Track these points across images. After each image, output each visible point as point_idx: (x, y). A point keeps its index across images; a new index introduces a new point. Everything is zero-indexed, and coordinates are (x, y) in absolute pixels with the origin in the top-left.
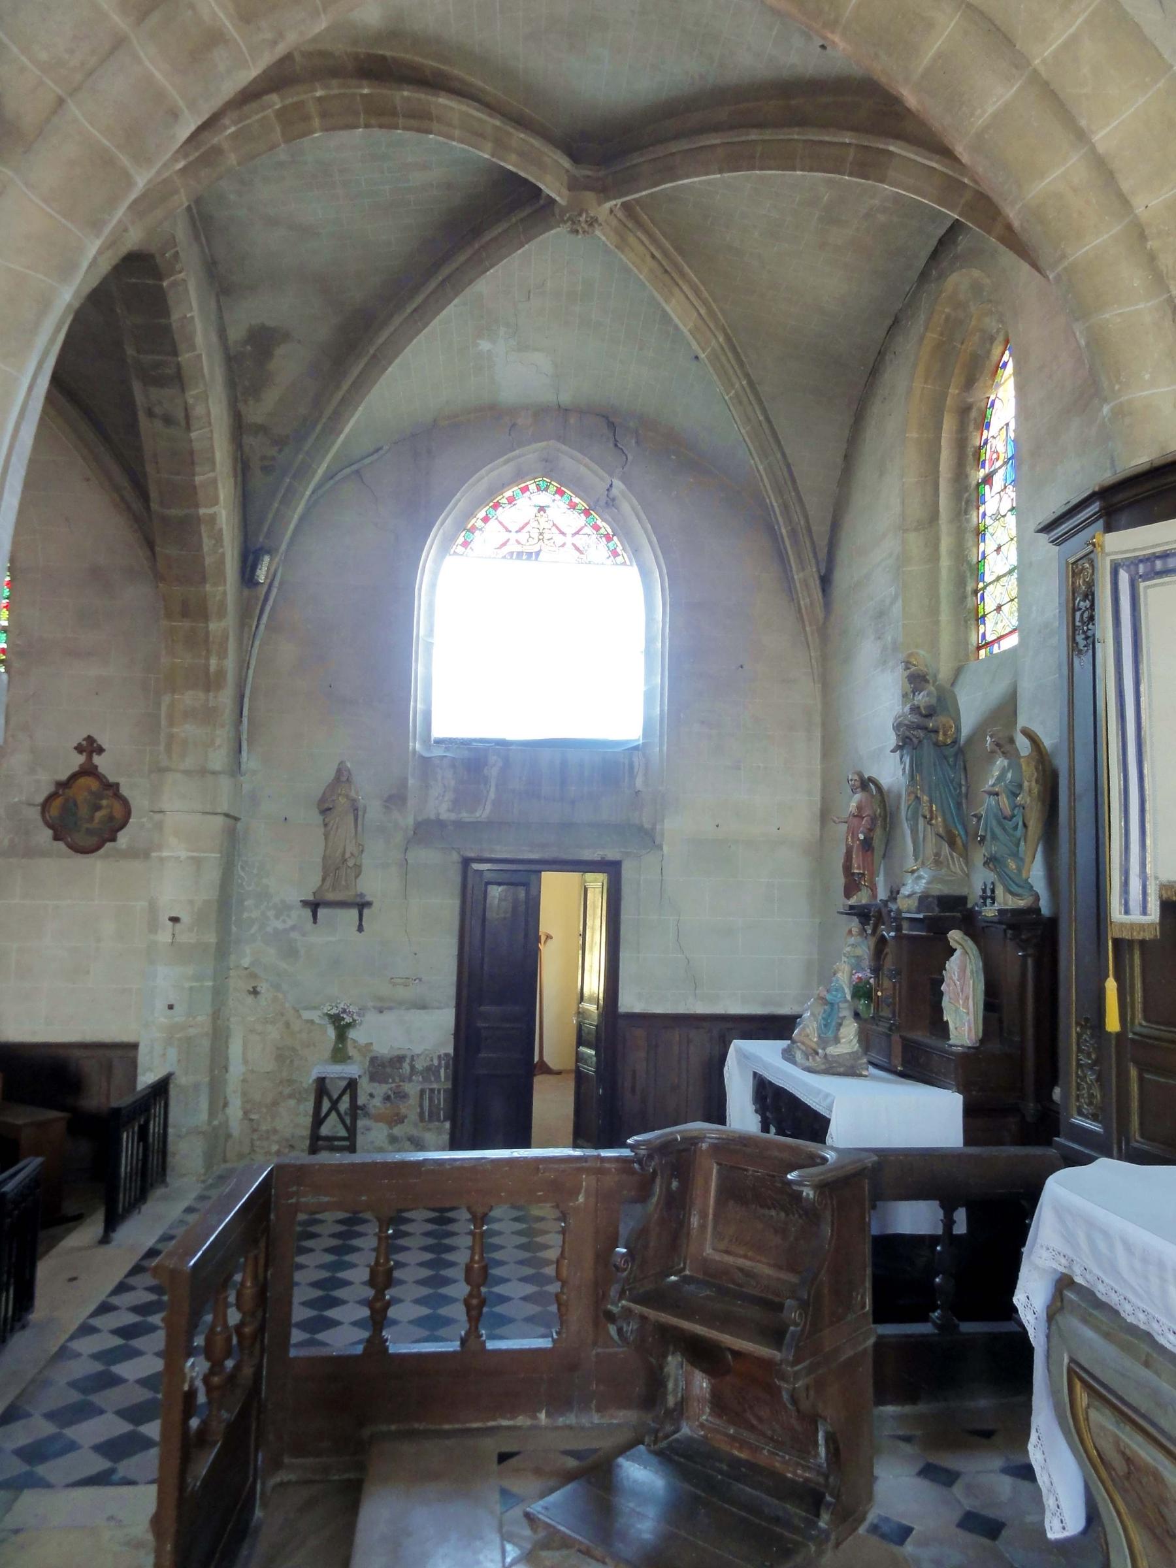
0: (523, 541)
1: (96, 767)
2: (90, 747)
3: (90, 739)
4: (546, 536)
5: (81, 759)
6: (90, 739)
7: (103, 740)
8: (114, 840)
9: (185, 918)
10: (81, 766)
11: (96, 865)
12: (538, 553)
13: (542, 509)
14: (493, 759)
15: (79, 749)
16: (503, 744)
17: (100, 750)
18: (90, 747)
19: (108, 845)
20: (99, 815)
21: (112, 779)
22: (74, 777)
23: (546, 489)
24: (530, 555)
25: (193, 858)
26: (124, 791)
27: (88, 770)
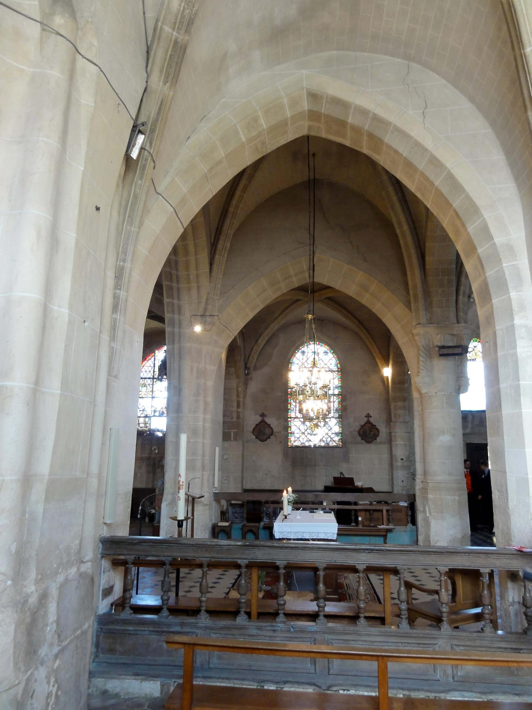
0: (471, 356)
1: (370, 421)
2: (368, 416)
3: (368, 414)
4: (477, 354)
5: (366, 419)
6: (368, 414)
7: (371, 414)
8: (376, 439)
9: (404, 459)
10: (367, 421)
11: (372, 446)
12: (475, 359)
13: (475, 347)
14: (469, 416)
15: (366, 417)
16: (471, 411)
17: (371, 417)
18: (368, 416)
19: (375, 441)
20: (372, 433)
21: (374, 424)
22: (365, 424)
23: (476, 341)
24: (473, 360)
25: (404, 444)
26: (377, 427)
27: (368, 422)
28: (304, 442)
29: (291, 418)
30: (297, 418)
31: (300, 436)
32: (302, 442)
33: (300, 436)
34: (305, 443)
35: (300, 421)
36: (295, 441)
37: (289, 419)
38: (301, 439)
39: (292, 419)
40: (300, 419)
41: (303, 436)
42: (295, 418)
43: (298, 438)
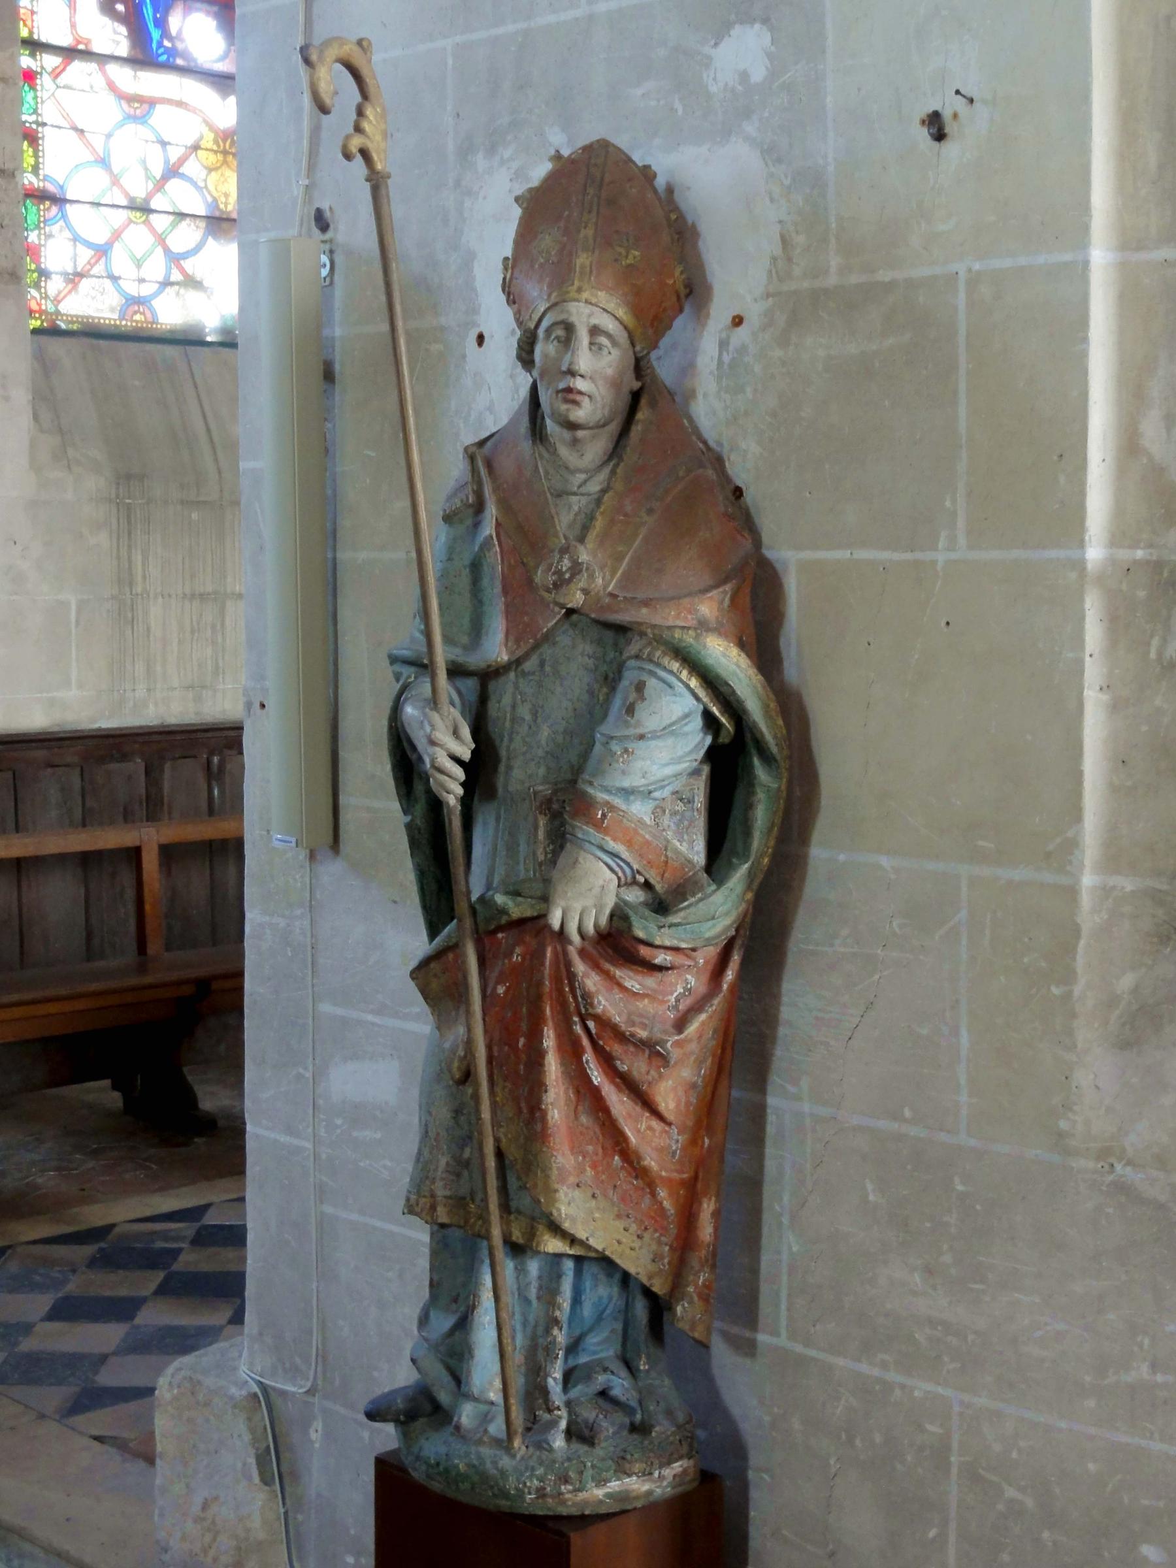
28: (146, 290)
29: (34, 46)
30: (87, 55)
31: (117, 235)
32: (133, 289)
33: (117, 235)
34: (156, 303)
35: (112, 86)
36: (75, 278)
37: (26, 61)
38: (120, 261)
39: (50, 61)
40: (113, 69)
41: (138, 237)
42: (70, 53)
43: (102, 251)
